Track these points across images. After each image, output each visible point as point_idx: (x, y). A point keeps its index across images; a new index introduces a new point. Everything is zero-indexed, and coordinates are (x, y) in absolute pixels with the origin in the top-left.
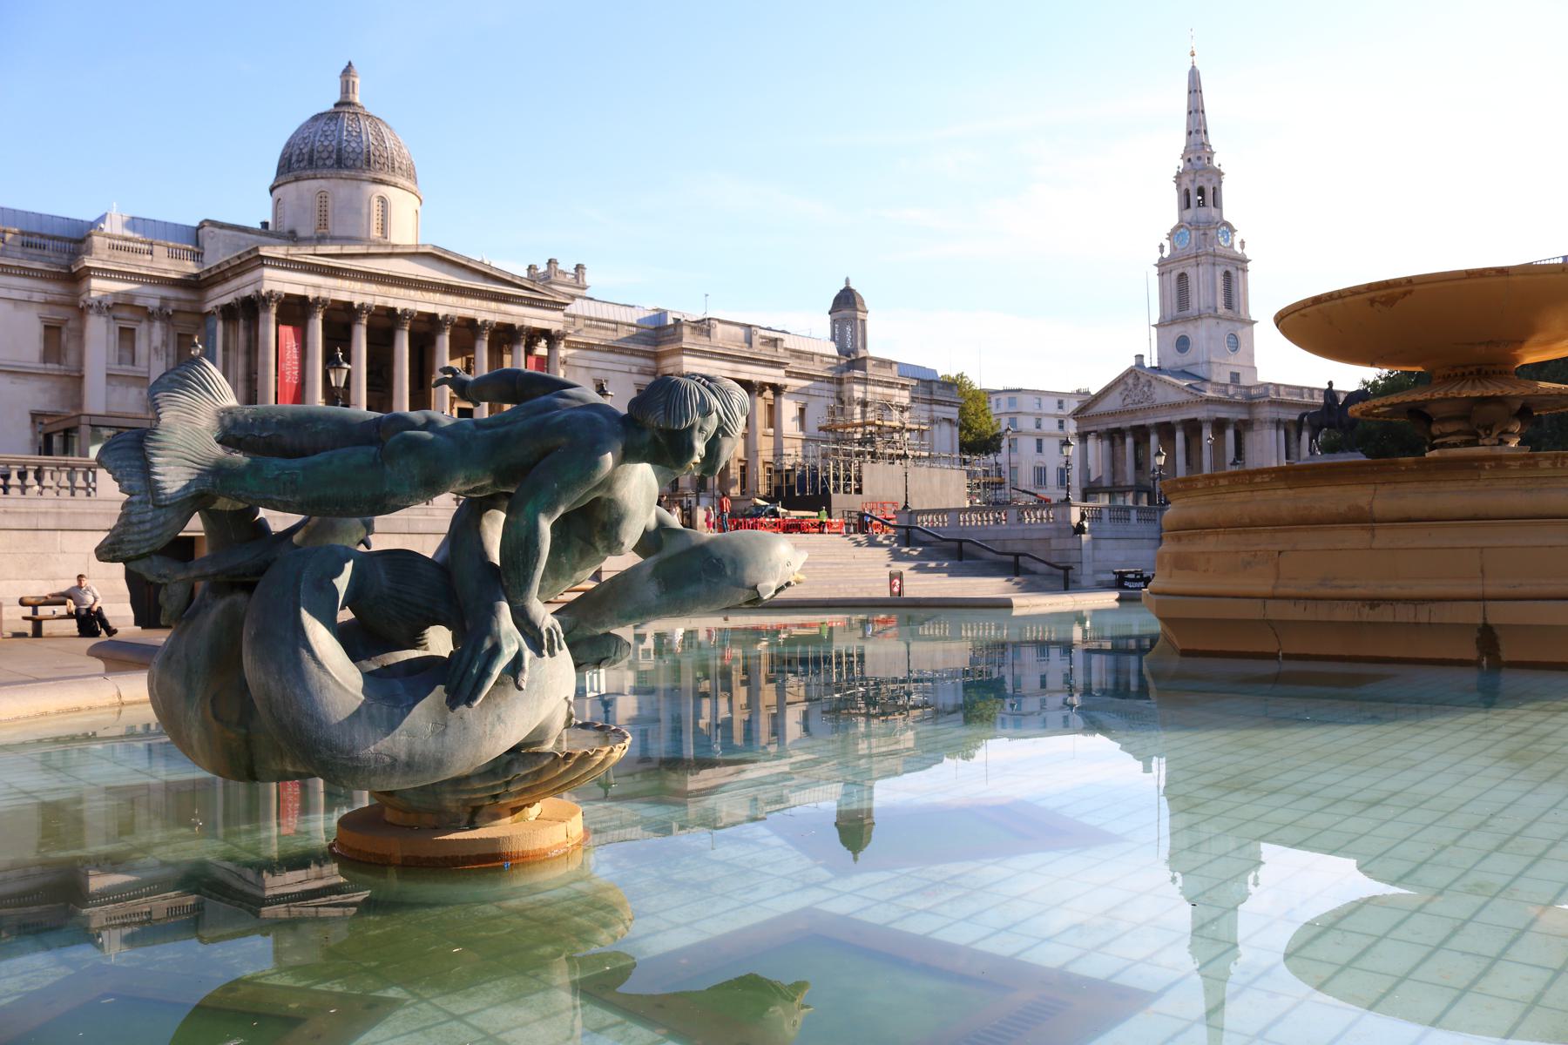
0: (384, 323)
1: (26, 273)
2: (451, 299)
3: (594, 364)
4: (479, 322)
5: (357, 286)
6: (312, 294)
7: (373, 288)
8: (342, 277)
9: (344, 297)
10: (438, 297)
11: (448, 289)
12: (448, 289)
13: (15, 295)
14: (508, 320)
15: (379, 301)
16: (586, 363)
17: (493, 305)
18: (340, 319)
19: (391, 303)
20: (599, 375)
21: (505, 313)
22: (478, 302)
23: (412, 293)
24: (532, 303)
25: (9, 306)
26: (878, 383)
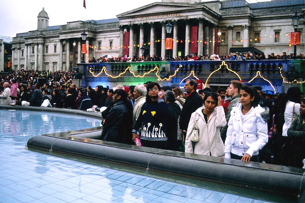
0: (147, 27)
2: (165, 16)
3: (274, 25)
6: (129, 24)
7: (145, 18)
8: (136, 18)
9: (136, 23)
13: (117, 36)
14: (183, 18)
15: (145, 22)
16: (270, 25)
18: (136, 28)
20: (277, 28)
23: (154, 17)
24: (190, 11)
25: (116, 38)
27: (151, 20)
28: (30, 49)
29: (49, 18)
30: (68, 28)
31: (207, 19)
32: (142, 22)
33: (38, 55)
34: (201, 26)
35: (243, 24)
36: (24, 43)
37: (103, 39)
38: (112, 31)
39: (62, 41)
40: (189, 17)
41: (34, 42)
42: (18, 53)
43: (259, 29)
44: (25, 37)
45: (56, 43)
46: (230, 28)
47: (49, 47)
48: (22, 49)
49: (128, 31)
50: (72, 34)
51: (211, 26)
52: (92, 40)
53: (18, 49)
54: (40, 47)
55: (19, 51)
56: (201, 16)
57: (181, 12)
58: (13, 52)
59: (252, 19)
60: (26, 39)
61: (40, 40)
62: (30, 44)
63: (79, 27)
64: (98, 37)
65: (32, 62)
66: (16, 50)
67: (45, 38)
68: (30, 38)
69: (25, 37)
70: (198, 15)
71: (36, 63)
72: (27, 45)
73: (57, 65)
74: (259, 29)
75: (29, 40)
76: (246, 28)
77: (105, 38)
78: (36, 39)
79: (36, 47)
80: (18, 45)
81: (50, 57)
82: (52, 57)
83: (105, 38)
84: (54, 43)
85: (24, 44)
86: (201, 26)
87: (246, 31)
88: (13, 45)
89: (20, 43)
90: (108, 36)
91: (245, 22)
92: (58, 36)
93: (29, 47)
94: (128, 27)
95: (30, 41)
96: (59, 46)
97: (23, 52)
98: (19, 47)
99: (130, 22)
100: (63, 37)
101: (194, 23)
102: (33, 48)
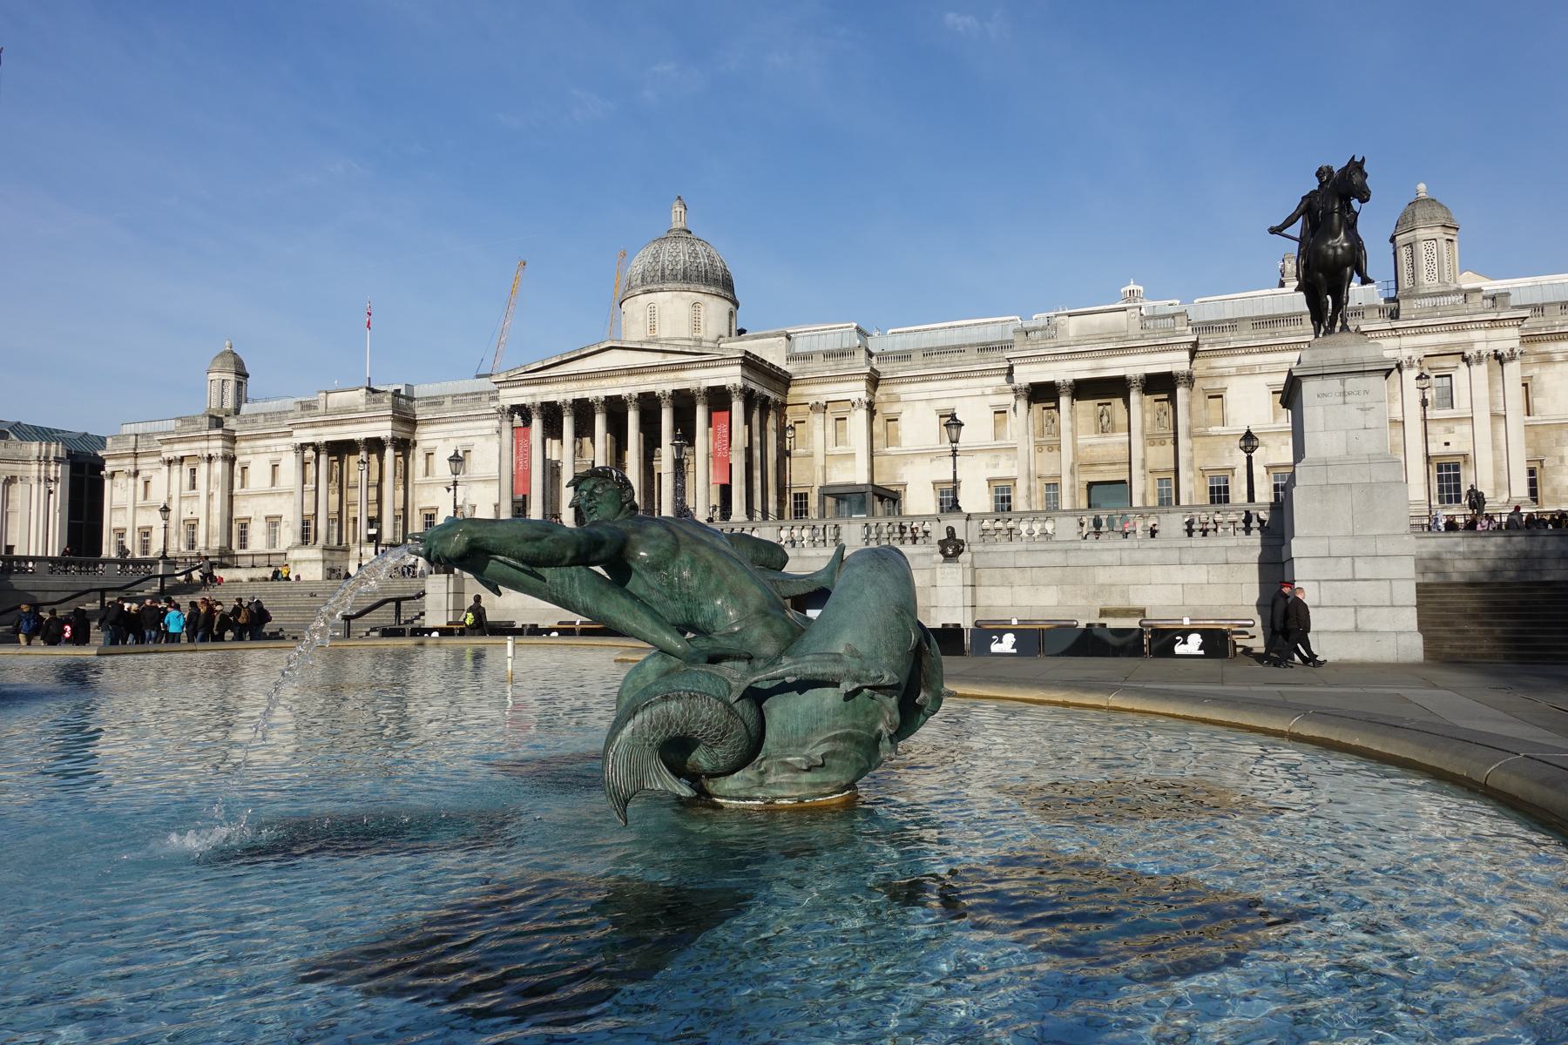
1: (488, 416)
2: (634, 380)
4: (658, 391)
5: (561, 387)
6: (527, 401)
10: (624, 380)
11: (631, 371)
12: (631, 371)
15: (578, 396)
17: (672, 375)
18: (551, 416)
19: (586, 395)
20: (945, 405)
21: (682, 380)
22: (658, 376)
23: (604, 382)
24: (706, 365)
25: (482, 440)
26: (1421, 330)
27: (596, 391)
28: (180, 475)
29: (247, 376)
30: (321, 409)
31: (752, 386)
32: (570, 398)
33: (210, 496)
34: (737, 406)
35: (854, 397)
36: (159, 454)
37: (439, 443)
38: (468, 418)
39: (303, 447)
40: (705, 384)
41: (199, 453)
42: (131, 488)
43: (895, 408)
44: (160, 433)
45: (276, 457)
46: (815, 408)
47: (251, 469)
48: (142, 474)
49: (527, 422)
50: (336, 429)
51: (765, 406)
52: (404, 446)
53: (129, 474)
54: (218, 467)
55: (131, 481)
56: (739, 382)
57: (681, 367)
58: (107, 483)
59: (874, 381)
60: (170, 442)
61: (216, 447)
62: (182, 459)
63: (362, 408)
64: (425, 437)
65: (188, 516)
66: (119, 479)
67: (232, 439)
68: (181, 440)
69: (160, 433)
70: (731, 376)
71: (202, 522)
72: (170, 462)
73: (283, 525)
74: (895, 408)
75: (176, 446)
76: (860, 406)
77: (446, 439)
78: (205, 444)
79: (202, 469)
80: (127, 461)
81: (254, 501)
82: (267, 500)
83: (446, 439)
84: (270, 456)
85: (156, 459)
86: (737, 406)
87: (861, 415)
88: (108, 463)
89: (136, 455)
90: (455, 434)
91: (857, 390)
92: (290, 434)
93: (176, 468)
94: (524, 412)
95: (180, 450)
96: (290, 463)
97: (147, 482)
98: (132, 470)
99: (533, 395)
100: (307, 436)
101: (718, 399)
102: (193, 471)
